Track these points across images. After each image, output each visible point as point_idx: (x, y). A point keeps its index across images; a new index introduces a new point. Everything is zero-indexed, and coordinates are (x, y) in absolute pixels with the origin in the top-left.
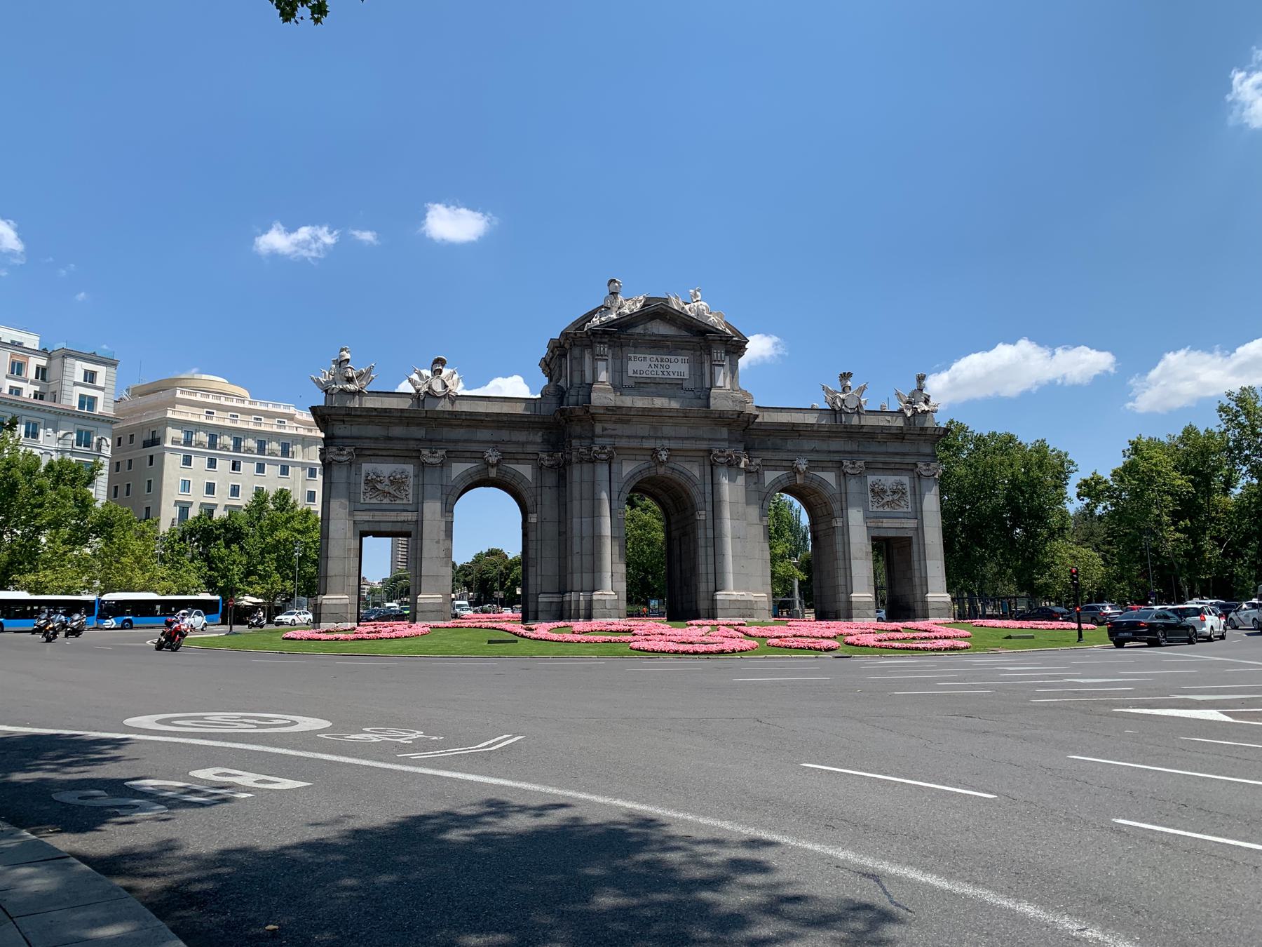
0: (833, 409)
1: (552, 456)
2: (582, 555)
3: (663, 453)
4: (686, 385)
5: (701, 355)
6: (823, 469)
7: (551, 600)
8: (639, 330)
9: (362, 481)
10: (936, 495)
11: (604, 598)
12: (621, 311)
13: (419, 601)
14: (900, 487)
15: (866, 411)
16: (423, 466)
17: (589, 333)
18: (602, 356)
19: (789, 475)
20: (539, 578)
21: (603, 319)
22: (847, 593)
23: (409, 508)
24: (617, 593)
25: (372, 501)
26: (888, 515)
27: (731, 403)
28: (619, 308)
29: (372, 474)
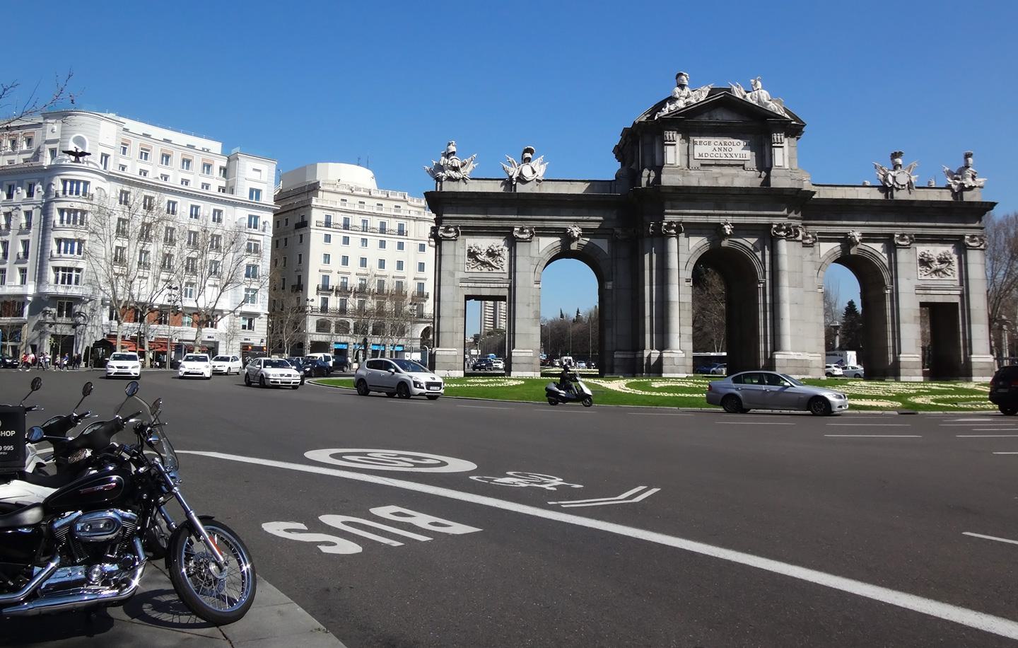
3: (725, 226)
7: (625, 356)
9: (466, 255)
11: (672, 355)
12: (687, 100)
13: (513, 354)
14: (947, 256)
15: (917, 188)
29: (474, 248)
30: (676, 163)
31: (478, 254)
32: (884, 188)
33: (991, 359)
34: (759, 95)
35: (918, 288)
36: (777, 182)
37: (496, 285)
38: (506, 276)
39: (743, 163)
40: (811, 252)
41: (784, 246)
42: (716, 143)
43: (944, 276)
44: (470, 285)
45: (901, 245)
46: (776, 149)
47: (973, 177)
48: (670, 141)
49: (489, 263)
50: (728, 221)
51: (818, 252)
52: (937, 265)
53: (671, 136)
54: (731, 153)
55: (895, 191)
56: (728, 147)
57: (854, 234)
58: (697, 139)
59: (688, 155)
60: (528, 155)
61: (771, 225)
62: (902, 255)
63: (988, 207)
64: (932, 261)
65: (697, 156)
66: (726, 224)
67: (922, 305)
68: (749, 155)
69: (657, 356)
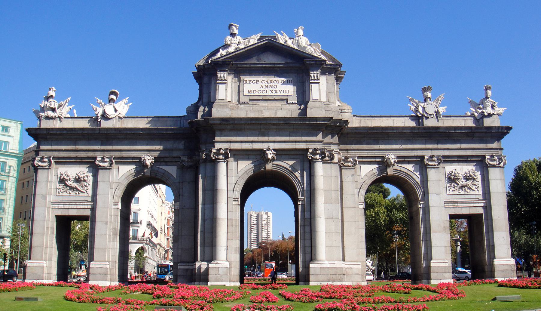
0: (417, 116)
1: (191, 158)
2: (204, 233)
3: (268, 152)
5: (303, 77)
6: (409, 162)
7: (187, 267)
8: (254, 61)
11: (217, 266)
14: (471, 174)
17: (213, 64)
19: (381, 168)
24: (230, 263)
25: (65, 194)
26: (462, 197)
27: (324, 112)
28: (238, 45)
29: (64, 175)
30: (226, 99)
31: (67, 180)
33: (512, 262)
34: (298, 40)
35: (447, 202)
36: (313, 112)
37: (82, 207)
38: (90, 199)
39: (286, 97)
41: (320, 168)
42: (263, 82)
43: (469, 191)
44: (60, 206)
45: (430, 165)
46: (313, 85)
47: (493, 107)
48: (221, 80)
51: (359, 173)
53: (222, 76)
54: (276, 89)
55: (424, 119)
56: (274, 84)
57: (390, 157)
58: (247, 78)
59: (239, 92)
60: (113, 97)
61: (307, 150)
62: (432, 174)
64: (459, 178)
66: (268, 149)
67: (452, 217)
68: (291, 89)
69: (206, 266)
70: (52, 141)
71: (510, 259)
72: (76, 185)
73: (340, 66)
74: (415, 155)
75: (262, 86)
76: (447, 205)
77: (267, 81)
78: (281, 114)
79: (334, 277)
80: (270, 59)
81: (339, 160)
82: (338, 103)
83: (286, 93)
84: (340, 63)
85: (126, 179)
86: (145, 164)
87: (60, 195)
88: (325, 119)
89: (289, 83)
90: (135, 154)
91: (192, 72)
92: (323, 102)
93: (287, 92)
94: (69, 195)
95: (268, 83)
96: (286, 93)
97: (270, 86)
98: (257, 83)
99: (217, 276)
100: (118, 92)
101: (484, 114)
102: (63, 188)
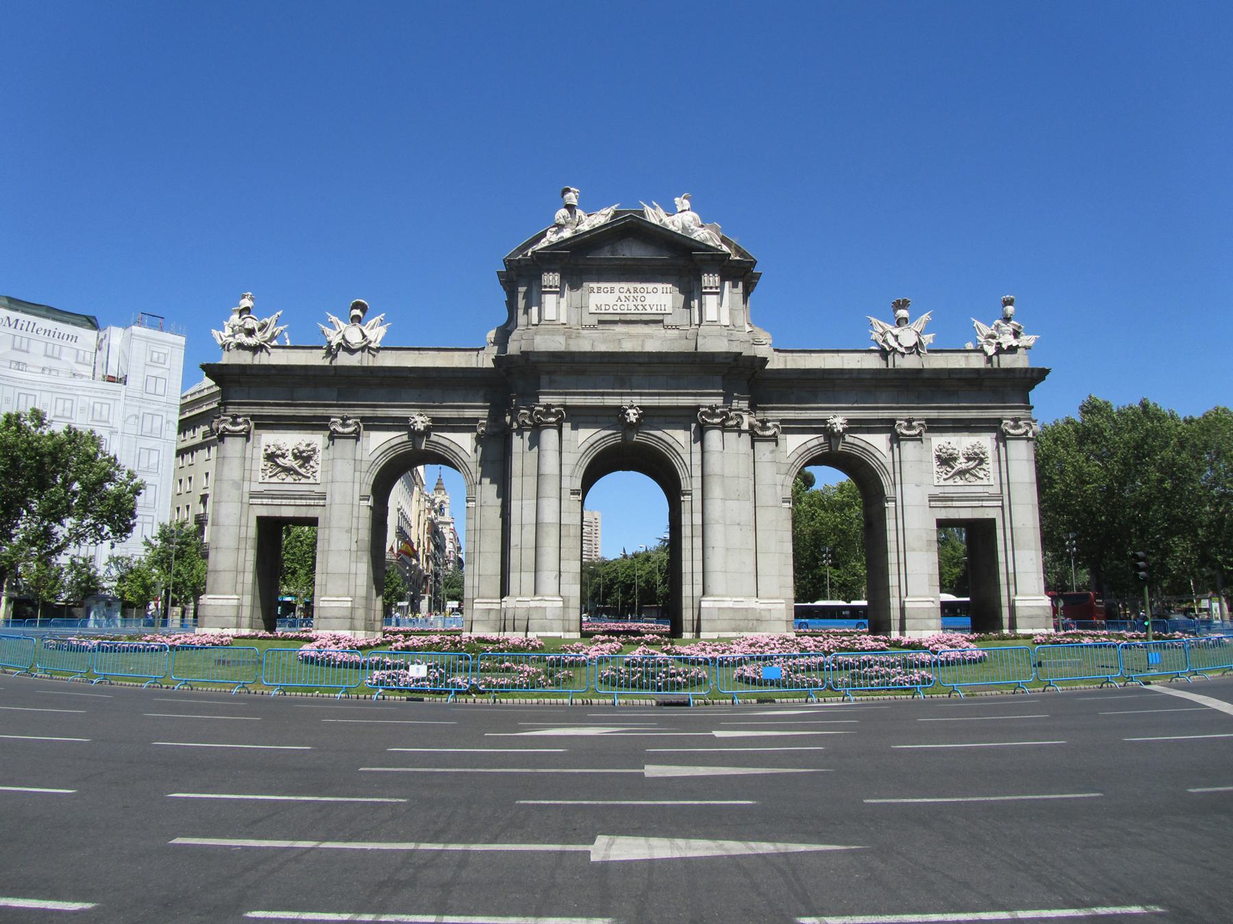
3: (629, 411)
4: (668, 320)
7: (489, 606)
8: (605, 254)
9: (262, 456)
10: (1028, 460)
14: (976, 450)
16: (334, 436)
18: (551, 287)
20: (476, 579)
21: (551, 240)
22: (900, 597)
23: (317, 489)
24: (565, 600)
28: (578, 225)
31: (278, 456)
32: (884, 353)
33: (1046, 601)
35: (933, 498)
37: (304, 502)
39: (660, 318)
40: (771, 449)
42: (622, 290)
43: (972, 479)
45: (906, 435)
46: (707, 296)
49: (292, 470)
50: (632, 404)
52: (961, 464)
54: (644, 303)
55: (896, 356)
56: (640, 295)
57: (835, 420)
58: (594, 285)
60: (357, 312)
63: (1035, 375)
65: (592, 309)
66: (631, 407)
67: (942, 524)
70: (250, 387)
71: (1042, 598)
72: (295, 464)
73: (754, 263)
74: (880, 418)
75: (619, 297)
76: (934, 503)
77: (628, 290)
78: (652, 346)
79: (742, 623)
80: (633, 251)
81: (751, 426)
82: (748, 329)
83: (661, 310)
84: (752, 258)
85: (382, 455)
86: (416, 429)
87: (265, 481)
88: (728, 355)
89: (667, 293)
90: (398, 413)
91: (498, 272)
92: (725, 326)
93: (663, 309)
94: (281, 481)
95: (630, 293)
96: (661, 310)
97: (634, 297)
98: (611, 292)
99: (541, 621)
100: (366, 303)
101: (1001, 346)
102: (270, 470)
